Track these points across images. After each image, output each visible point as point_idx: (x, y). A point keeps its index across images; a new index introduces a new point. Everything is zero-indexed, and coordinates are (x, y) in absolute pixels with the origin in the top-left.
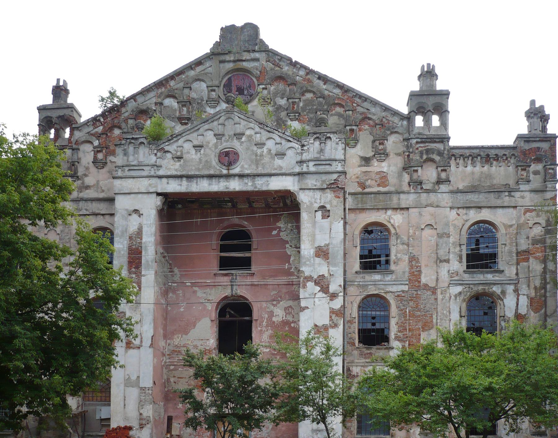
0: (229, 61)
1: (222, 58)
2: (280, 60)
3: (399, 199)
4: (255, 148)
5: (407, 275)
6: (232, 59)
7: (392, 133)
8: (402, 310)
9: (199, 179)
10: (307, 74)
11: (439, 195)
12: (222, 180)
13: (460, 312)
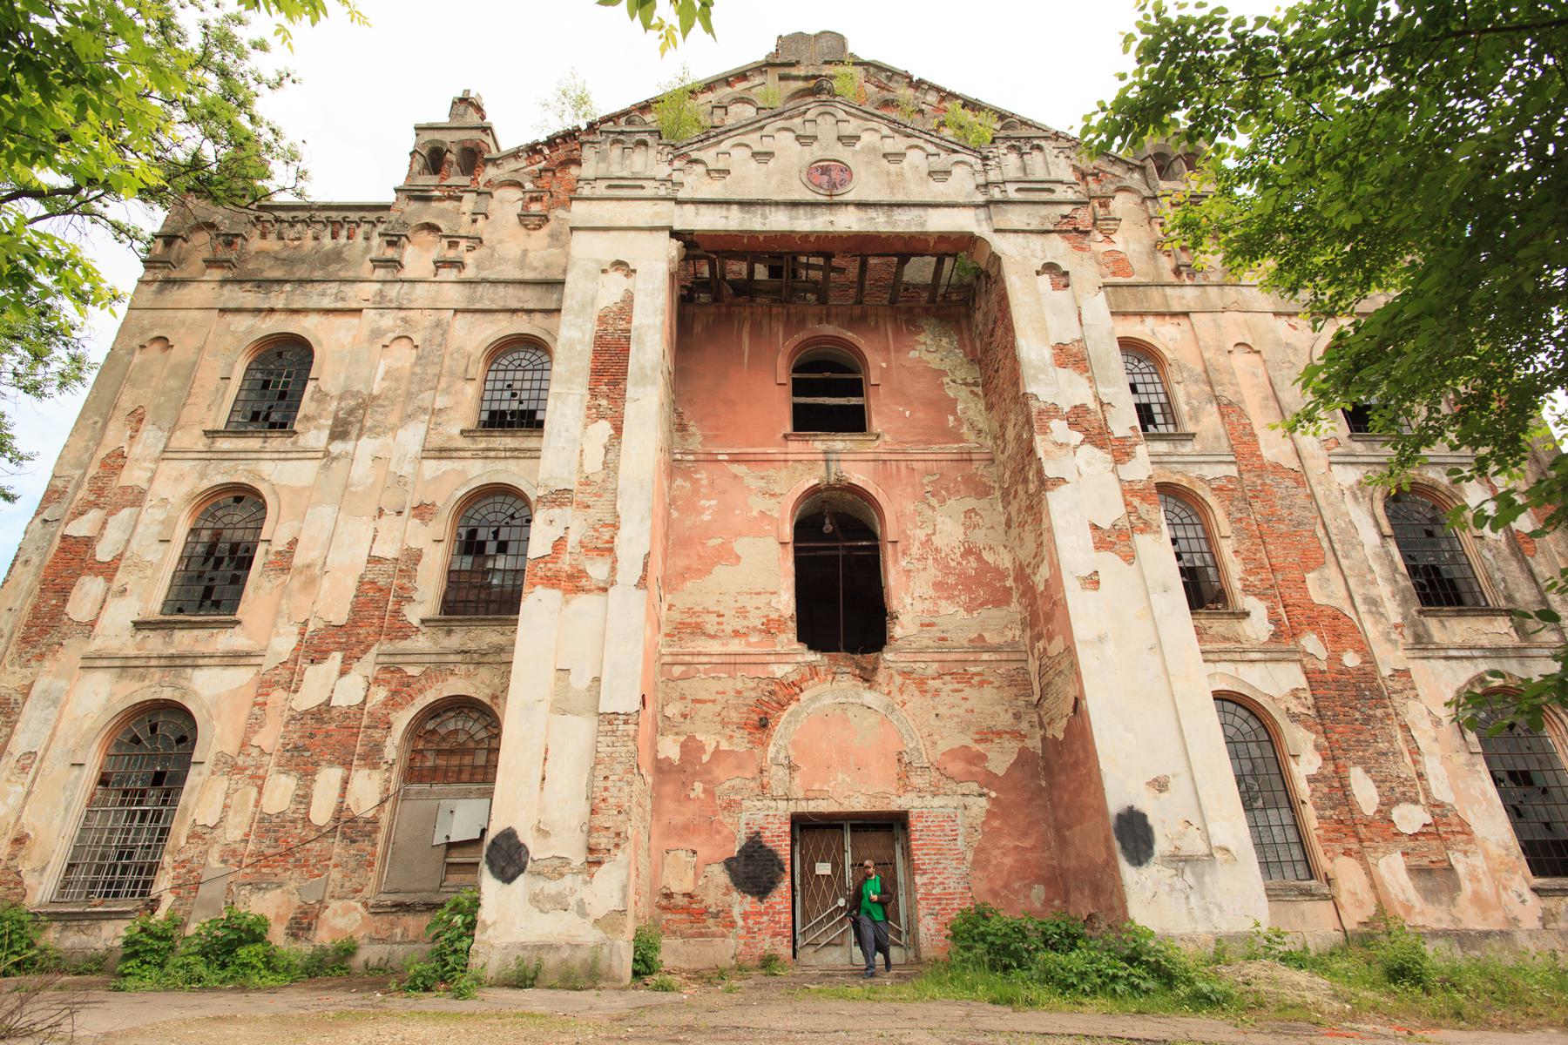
0: (796, 78)
1: (786, 71)
2: (890, 79)
3: (1165, 296)
4: (884, 161)
5: (1224, 443)
6: (802, 73)
7: (1119, 189)
8: (1240, 520)
9: (767, 209)
10: (943, 99)
11: (1244, 290)
12: (818, 211)
13: (1377, 524)
